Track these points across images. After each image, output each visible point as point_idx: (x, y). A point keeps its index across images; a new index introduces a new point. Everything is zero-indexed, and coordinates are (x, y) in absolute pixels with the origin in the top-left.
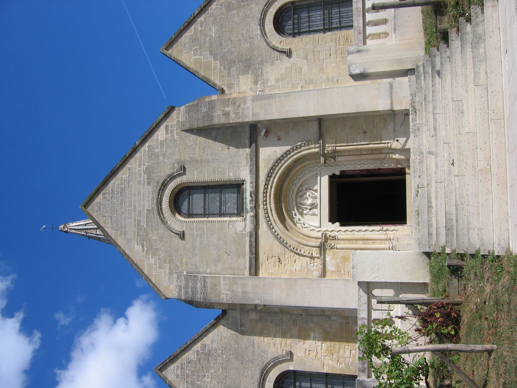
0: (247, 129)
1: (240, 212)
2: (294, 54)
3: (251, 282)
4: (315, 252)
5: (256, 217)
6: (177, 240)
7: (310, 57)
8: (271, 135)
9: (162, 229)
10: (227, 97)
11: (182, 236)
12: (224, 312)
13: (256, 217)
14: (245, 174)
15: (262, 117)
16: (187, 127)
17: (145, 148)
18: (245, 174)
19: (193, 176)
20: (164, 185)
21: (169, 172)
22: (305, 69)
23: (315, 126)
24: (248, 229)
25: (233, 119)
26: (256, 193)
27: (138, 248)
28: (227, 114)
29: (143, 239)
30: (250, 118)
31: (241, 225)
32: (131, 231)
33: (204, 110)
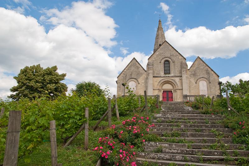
0: (181, 75)
1: (165, 74)
2: (196, 84)
3: (152, 76)
4: (158, 88)
5: (164, 77)
6: (159, 61)
7: (195, 87)
8: (179, 80)
9: (161, 58)
10: (187, 71)
11: (160, 62)
12: (146, 71)
13: (164, 77)
14: (172, 75)
15: (183, 78)
16: (182, 63)
17: (179, 55)
18: (172, 75)
19: (172, 64)
20: (170, 58)
21: (173, 59)
22: (193, 86)
23: (181, 88)
24: (162, 76)
25: (183, 72)
26: (169, 77)
27: (157, 53)
28: (184, 71)
29: (160, 54)
30: (183, 76)
31: (162, 74)
32: (161, 52)
33: (185, 67)
